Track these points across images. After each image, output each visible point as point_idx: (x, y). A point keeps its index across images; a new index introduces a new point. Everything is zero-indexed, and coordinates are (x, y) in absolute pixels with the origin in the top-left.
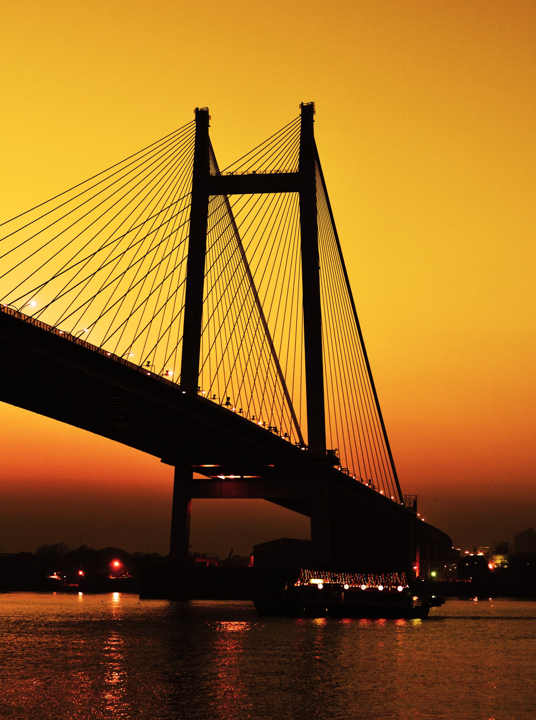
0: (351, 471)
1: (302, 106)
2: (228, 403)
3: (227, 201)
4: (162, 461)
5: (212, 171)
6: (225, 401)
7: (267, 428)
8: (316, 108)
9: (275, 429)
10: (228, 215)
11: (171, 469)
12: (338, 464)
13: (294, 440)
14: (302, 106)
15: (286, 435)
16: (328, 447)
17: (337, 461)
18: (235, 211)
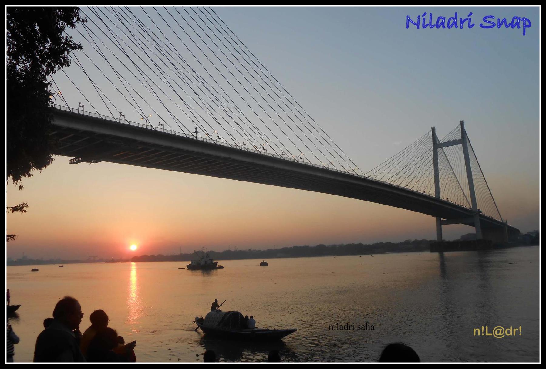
0: (486, 214)
1: (461, 122)
2: (447, 200)
3: (443, 149)
4: (433, 216)
5: (437, 141)
6: (447, 199)
7: (459, 205)
8: (465, 121)
9: (462, 205)
10: (446, 154)
11: (435, 218)
12: (481, 213)
13: (468, 207)
14: (461, 122)
15: (465, 207)
16: (478, 209)
17: (481, 212)
18: (446, 153)
